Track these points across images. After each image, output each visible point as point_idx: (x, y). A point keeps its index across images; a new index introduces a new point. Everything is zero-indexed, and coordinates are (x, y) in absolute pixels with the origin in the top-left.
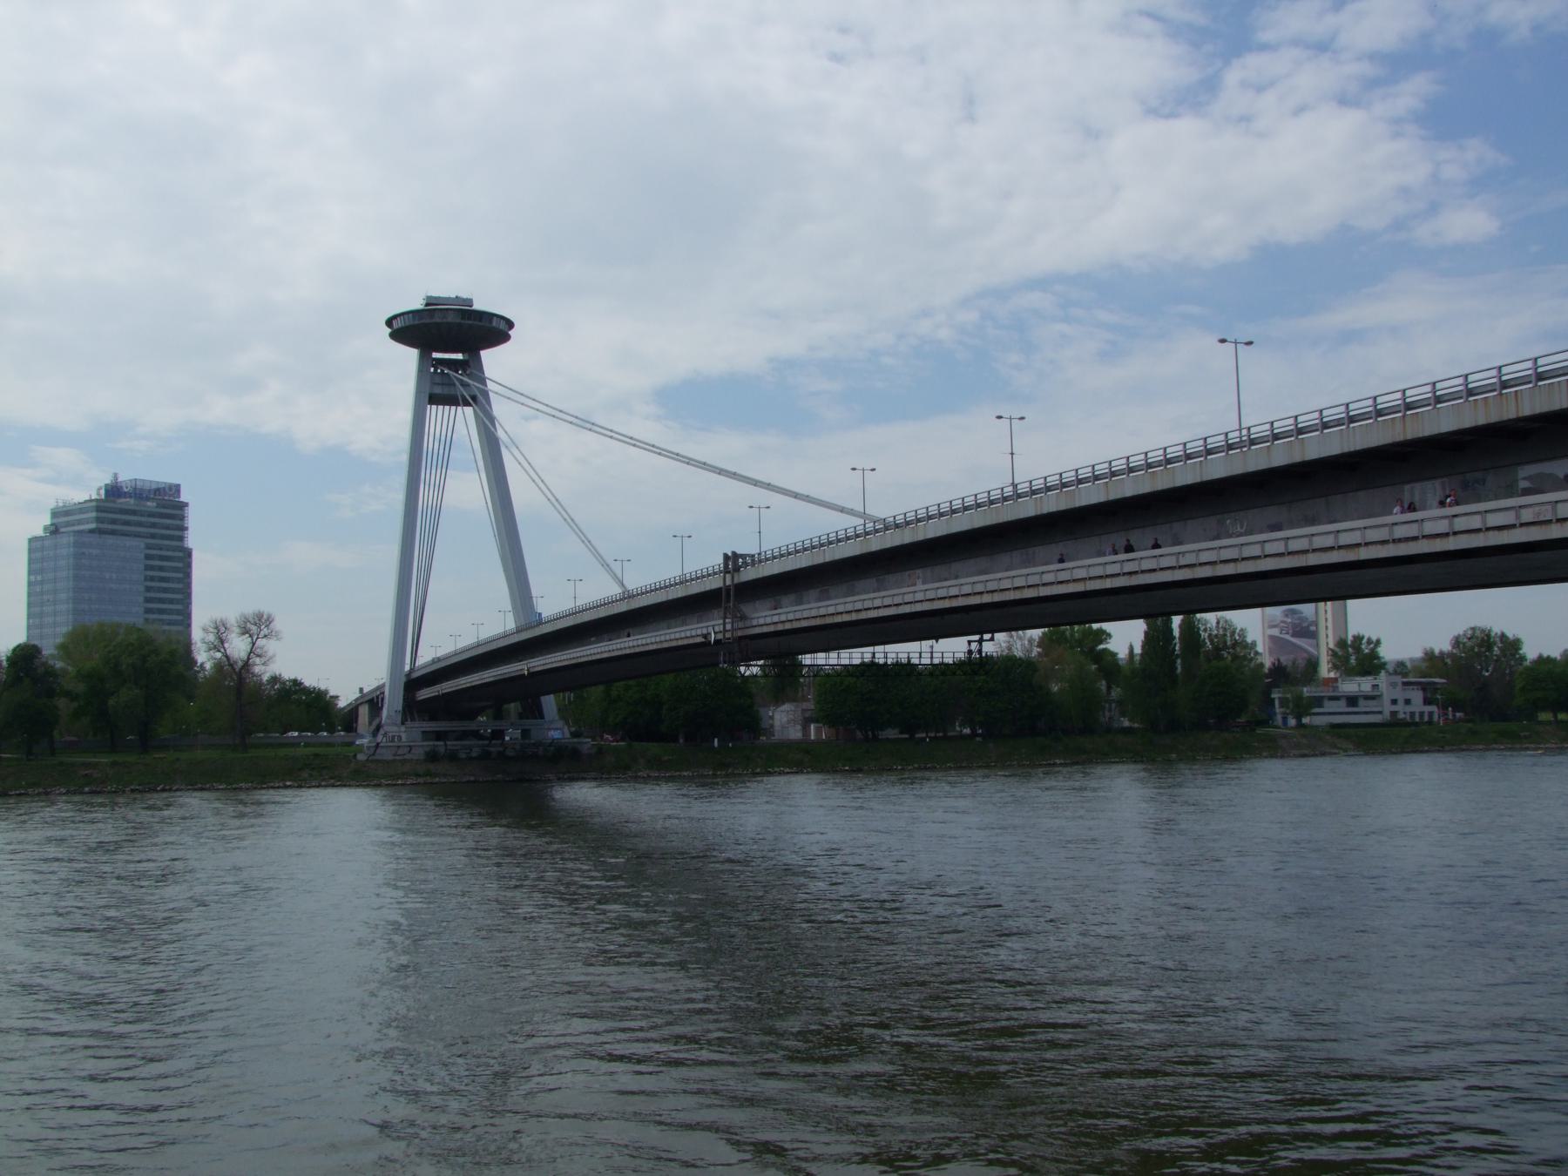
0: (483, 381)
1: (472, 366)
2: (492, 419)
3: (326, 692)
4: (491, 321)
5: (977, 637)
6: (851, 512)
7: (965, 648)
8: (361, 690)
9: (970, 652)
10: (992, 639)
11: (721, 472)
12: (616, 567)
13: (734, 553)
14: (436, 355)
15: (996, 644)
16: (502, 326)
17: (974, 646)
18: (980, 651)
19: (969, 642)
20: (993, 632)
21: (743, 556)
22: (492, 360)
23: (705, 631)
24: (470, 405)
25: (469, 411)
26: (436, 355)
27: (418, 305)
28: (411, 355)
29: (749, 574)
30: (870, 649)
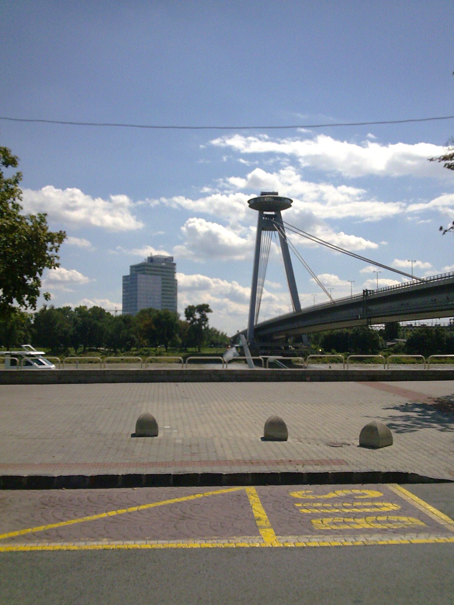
0: (282, 222)
1: (278, 217)
7: (449, 321)
8: (238, 331)
13: (366, 290)
14: (265, 213)
16: (289, 201)
19: (450, 320)
21: (370, 291)
24: (276, 230)
25: (277, 232)
26: (265, 213)
28: (256, 212)
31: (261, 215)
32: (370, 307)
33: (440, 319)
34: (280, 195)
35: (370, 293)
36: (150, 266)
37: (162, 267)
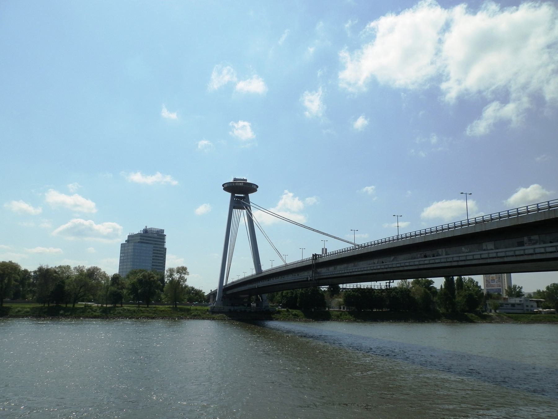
0: (249, 203)
1: (246, 199)
2: (251, 214)
3: (201, 291)
4: (252, 186)
5: (389, 281)
6: (351, 243)
8: (211, 290)
9: (386, 286)
10: (393, 282)
11: (314, 230)
12: (284, 257)
15: (396, 284)
16: (255, 187)
17: (388, 284)
18: (389, 286)
19: (386, 283)
20: (393, 280)
21: (318, 255)
22: (252, 197)
23: (307, 277)
25: (245, 211)
27: (232, 181)
28: (229, 195)
29: (321, 260)
30: (356, 284)
31: (233, 196)
32: (319, 270)
33: (377, 282)
34: (248, 181)
35: (319, 257)
36: (145, 237)
37: (154, 238)
